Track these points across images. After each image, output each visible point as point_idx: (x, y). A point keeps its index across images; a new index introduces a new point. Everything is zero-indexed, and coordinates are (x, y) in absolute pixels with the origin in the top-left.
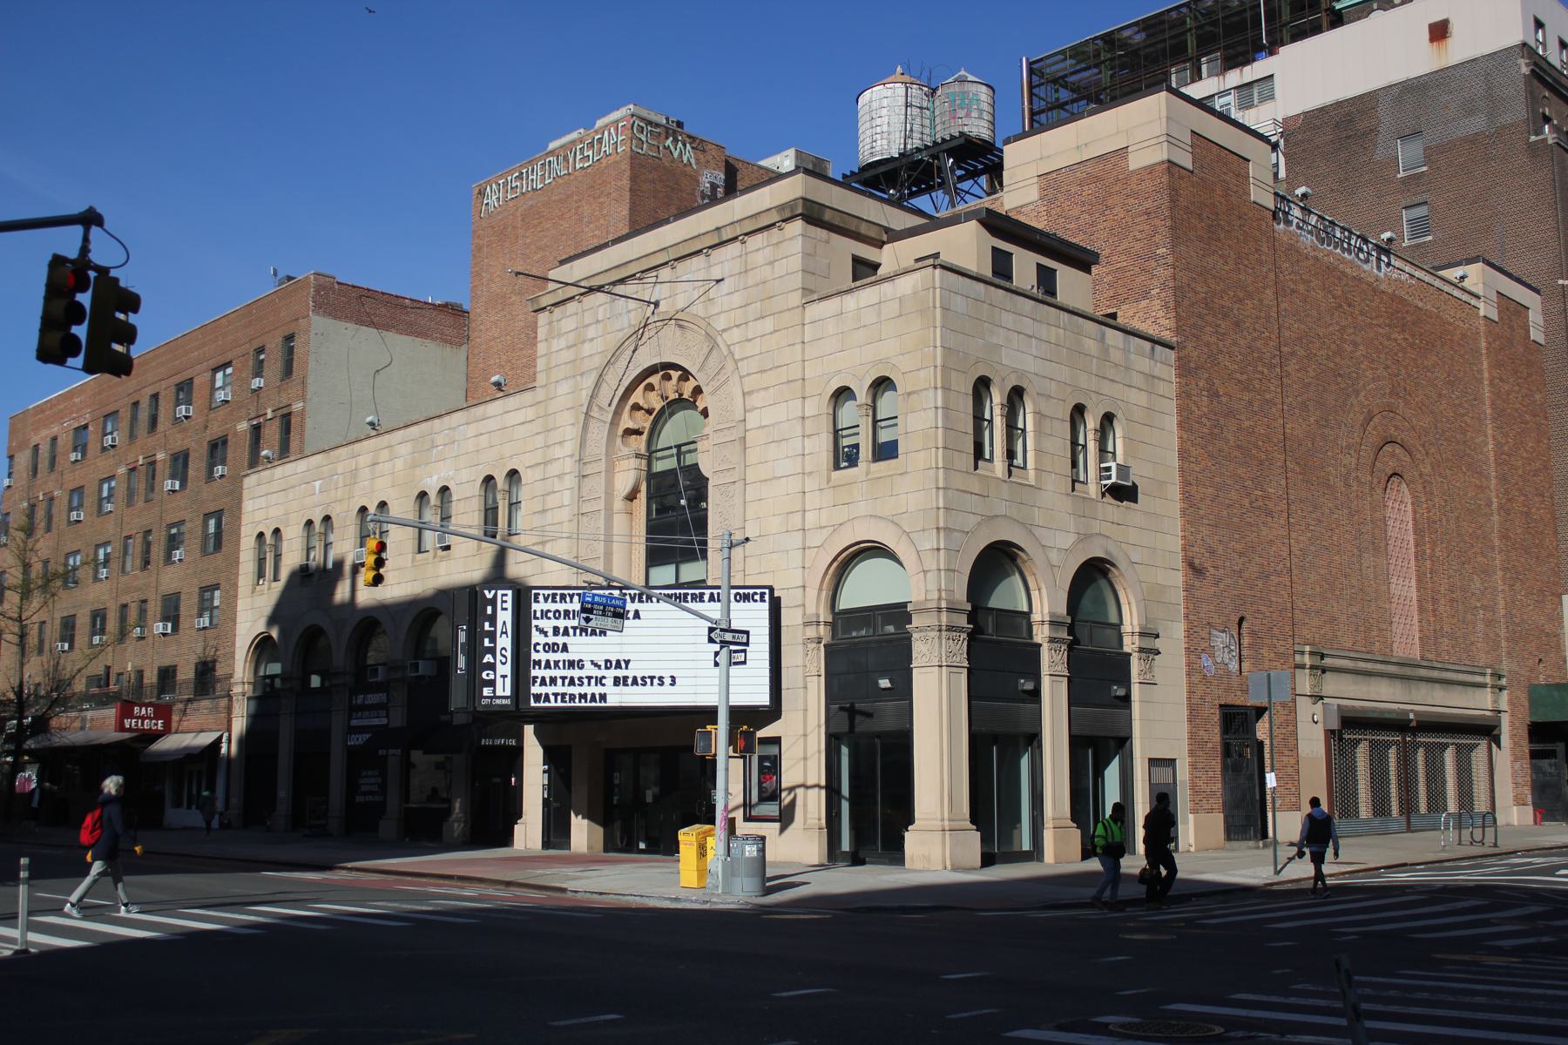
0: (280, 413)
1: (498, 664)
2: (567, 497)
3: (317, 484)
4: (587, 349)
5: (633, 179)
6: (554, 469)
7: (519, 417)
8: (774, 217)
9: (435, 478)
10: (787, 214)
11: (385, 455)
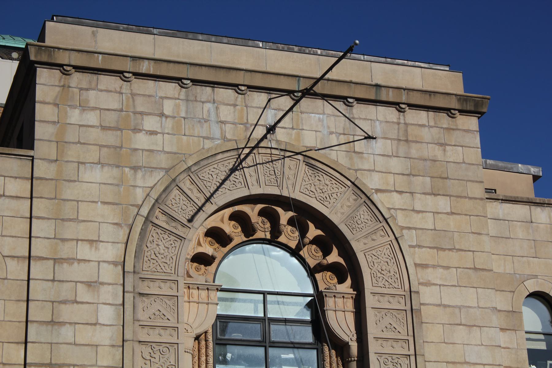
2: (107, 315)
4: (141, 141)
8: (453, 104)
10: (470, 107)
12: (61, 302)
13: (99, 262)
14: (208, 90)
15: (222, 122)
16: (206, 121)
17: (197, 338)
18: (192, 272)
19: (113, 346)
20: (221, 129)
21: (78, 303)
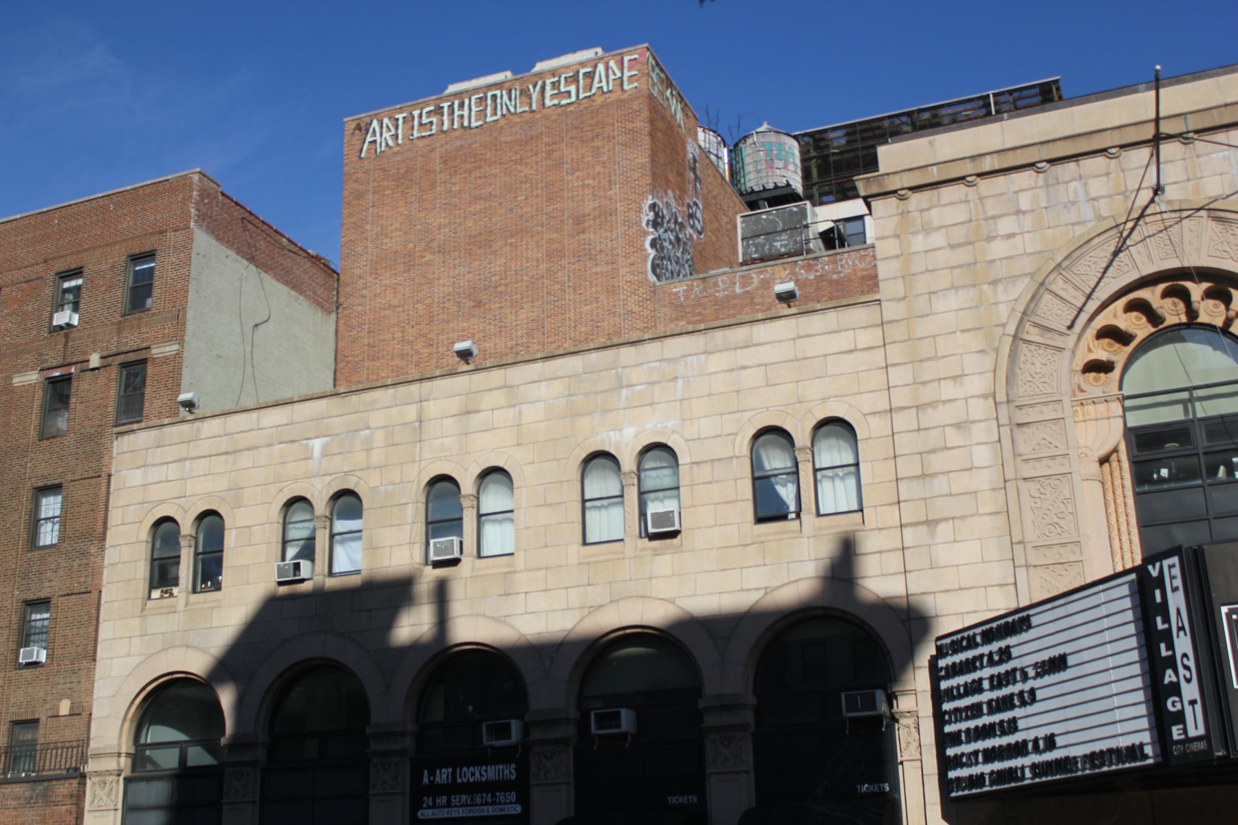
2: (983, 455)
3: (317, 445)
4: (998, 249)
5: (652, 121)
7: (843, 341)
9: (629, 432)
11: (499, 397)
12: (930, 452)
13: (966, 399)
14: (1072, 165)
15: (1094, 199)
16: (1073, 203)
17: (1104, 460)
18: (1084, 386)
19: (994, 489)
20: (1094, 208)
21: (948, 449)
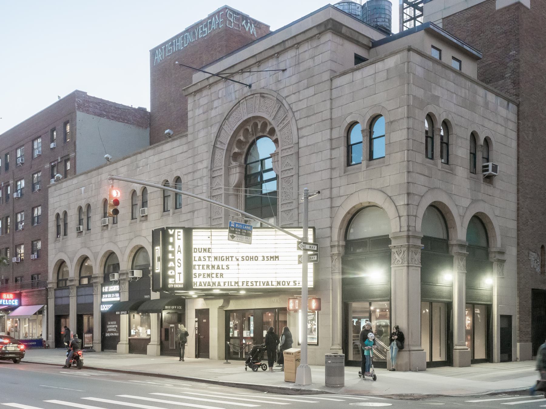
0: (64, 158)
1: (177, 267)
4: (213, 113)
6: (198, 175)
